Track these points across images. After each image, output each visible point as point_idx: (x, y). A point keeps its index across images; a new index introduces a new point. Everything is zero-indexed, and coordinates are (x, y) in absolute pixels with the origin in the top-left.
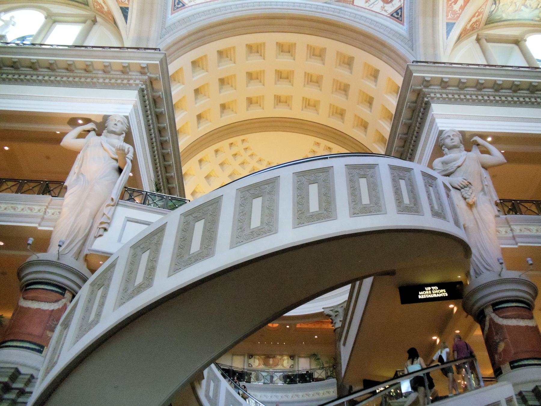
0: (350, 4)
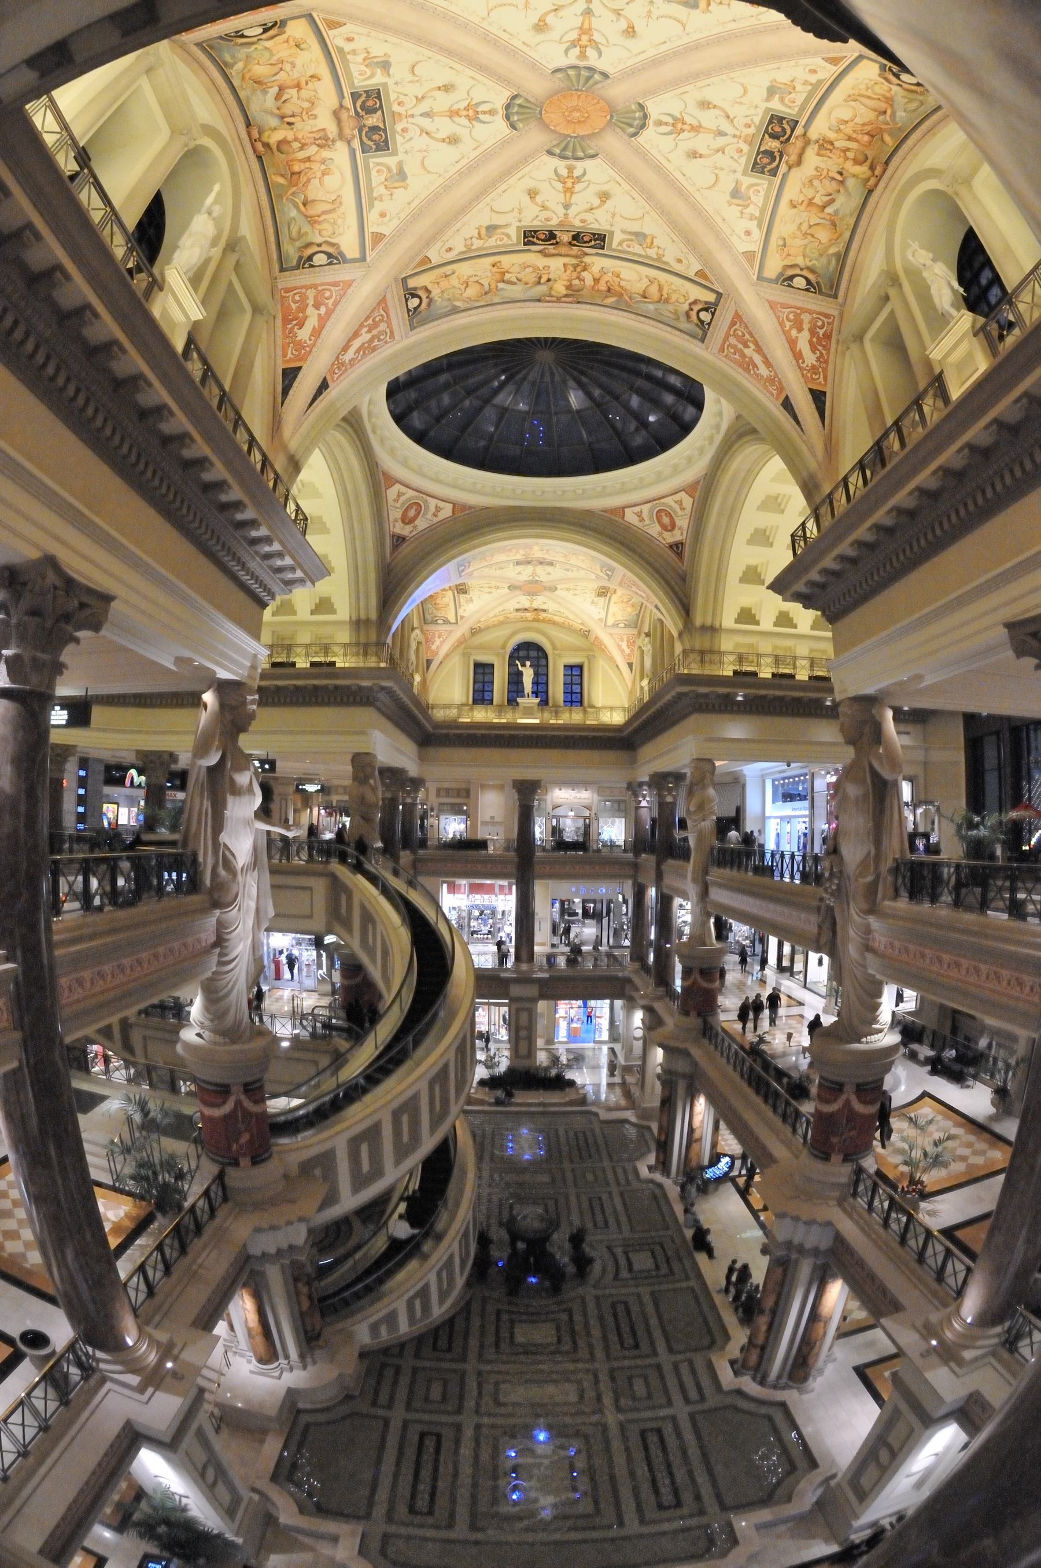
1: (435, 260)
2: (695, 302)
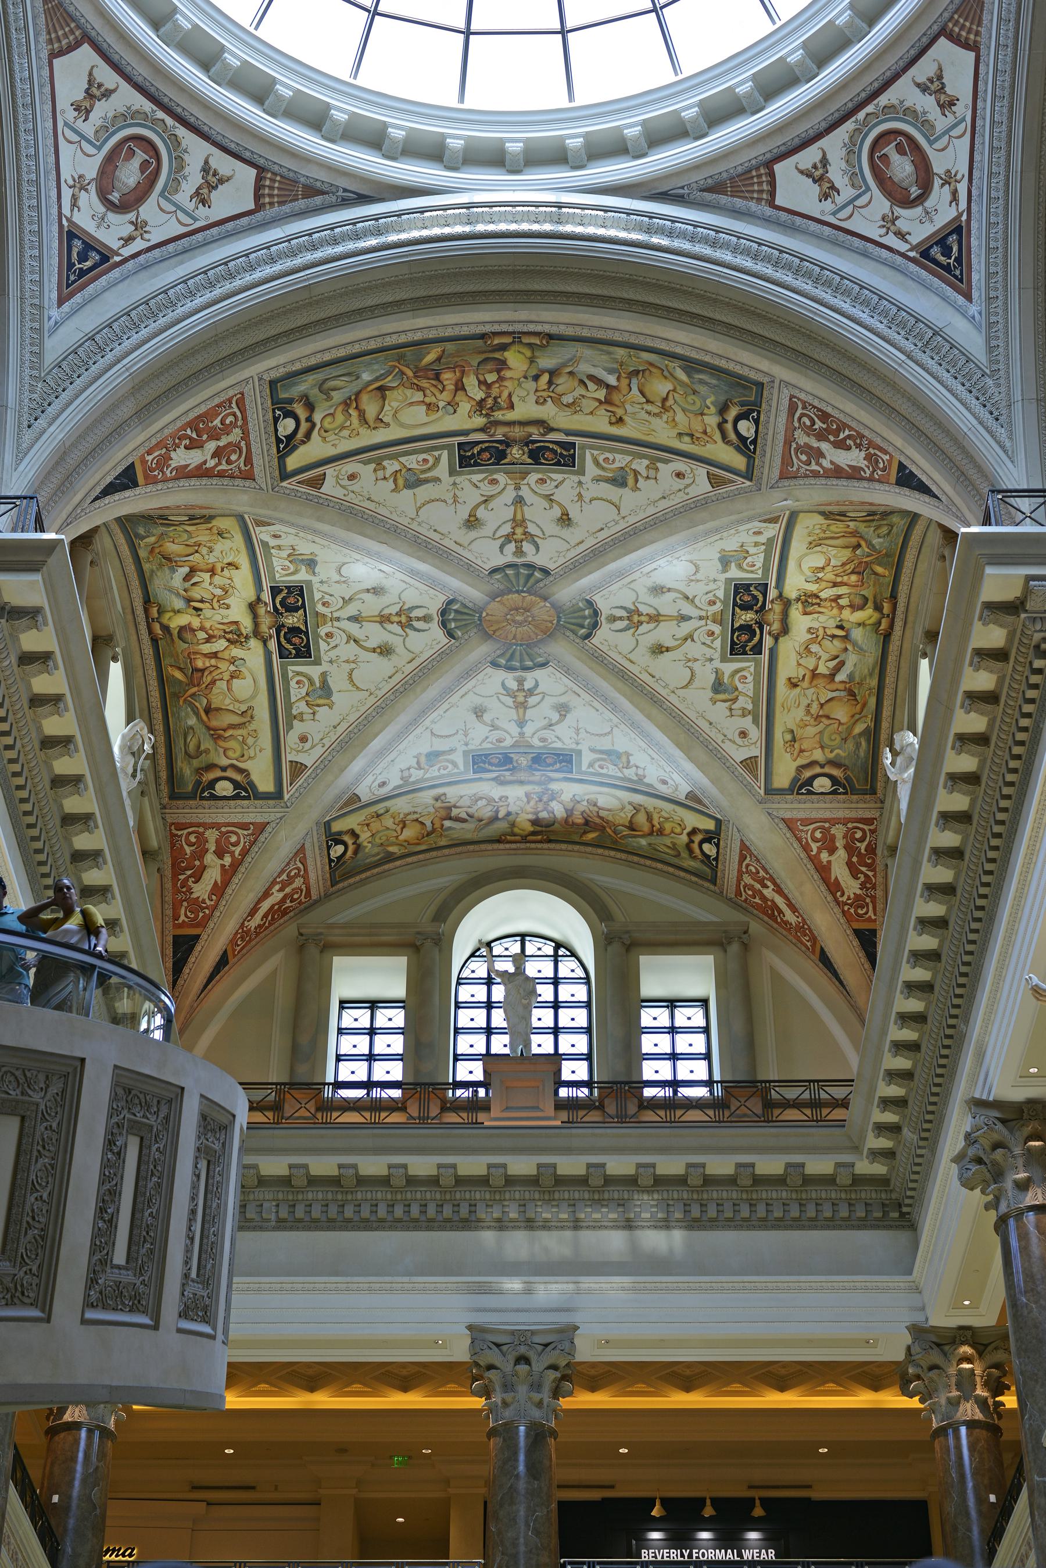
0: (50, 41)
1: (365, 798)
2: (694, 831)
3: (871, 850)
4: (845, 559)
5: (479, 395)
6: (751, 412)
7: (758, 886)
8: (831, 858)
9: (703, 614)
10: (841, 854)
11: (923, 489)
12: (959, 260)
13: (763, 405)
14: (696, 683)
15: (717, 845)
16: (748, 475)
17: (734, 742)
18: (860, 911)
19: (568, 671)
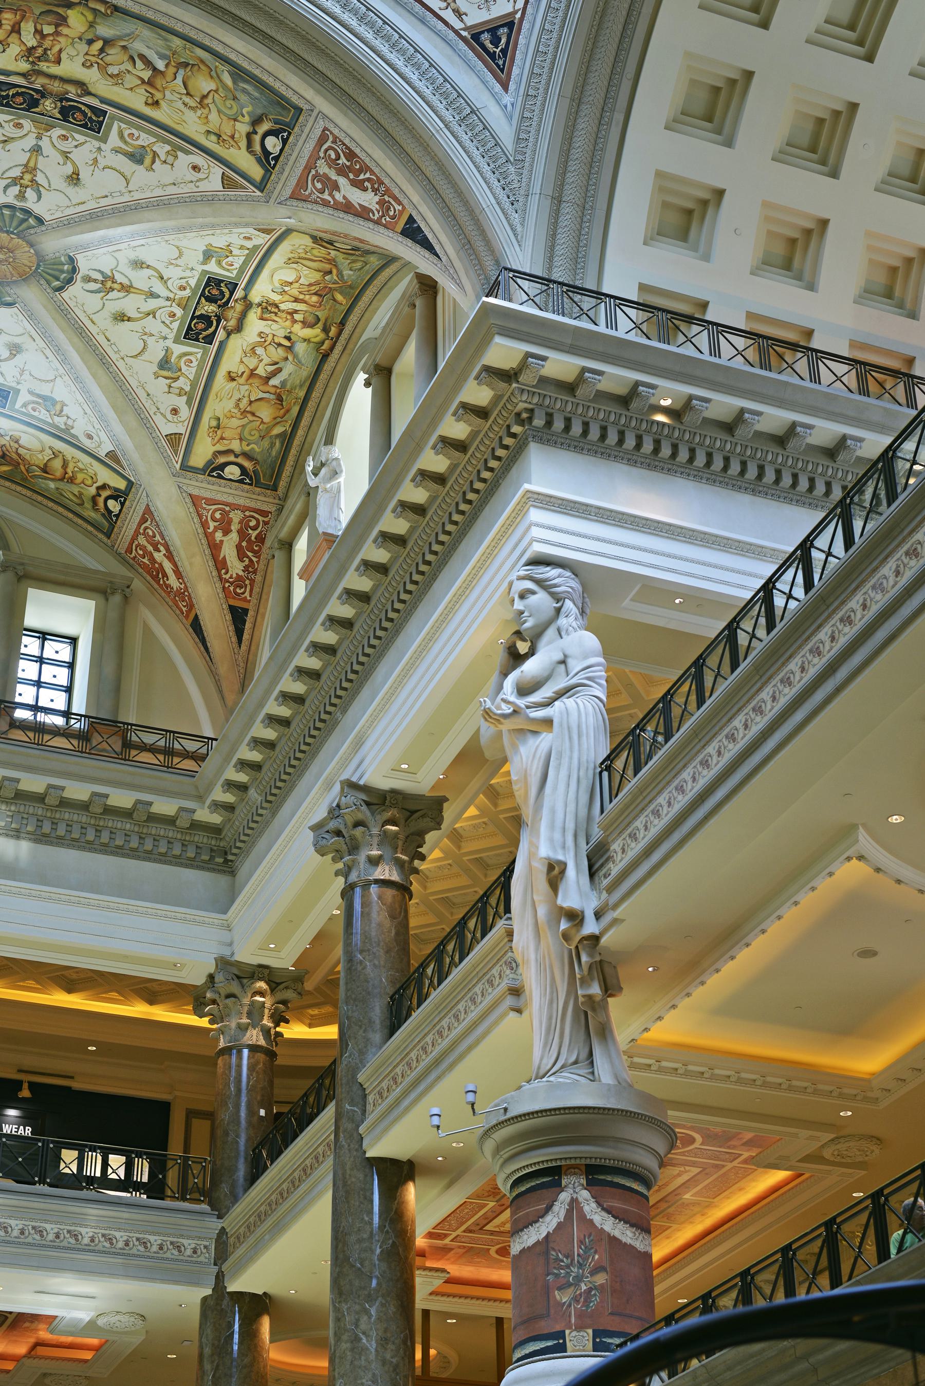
2: (104, 487)
3: (261, 539)
4: (313, 281)
5: (31, 42)
6: (281, 131)
7: (150, 548)
8: (225, 539)
9: (172, 296)
10: (234, 536)
11: (426, 245)
12: (504, 52)
13: (296, 129)
14: (146, 356)
15: (122, 504)
16: (261, 187)
17: (165, 417)
18: (238, 591)
19: (31, 316)
